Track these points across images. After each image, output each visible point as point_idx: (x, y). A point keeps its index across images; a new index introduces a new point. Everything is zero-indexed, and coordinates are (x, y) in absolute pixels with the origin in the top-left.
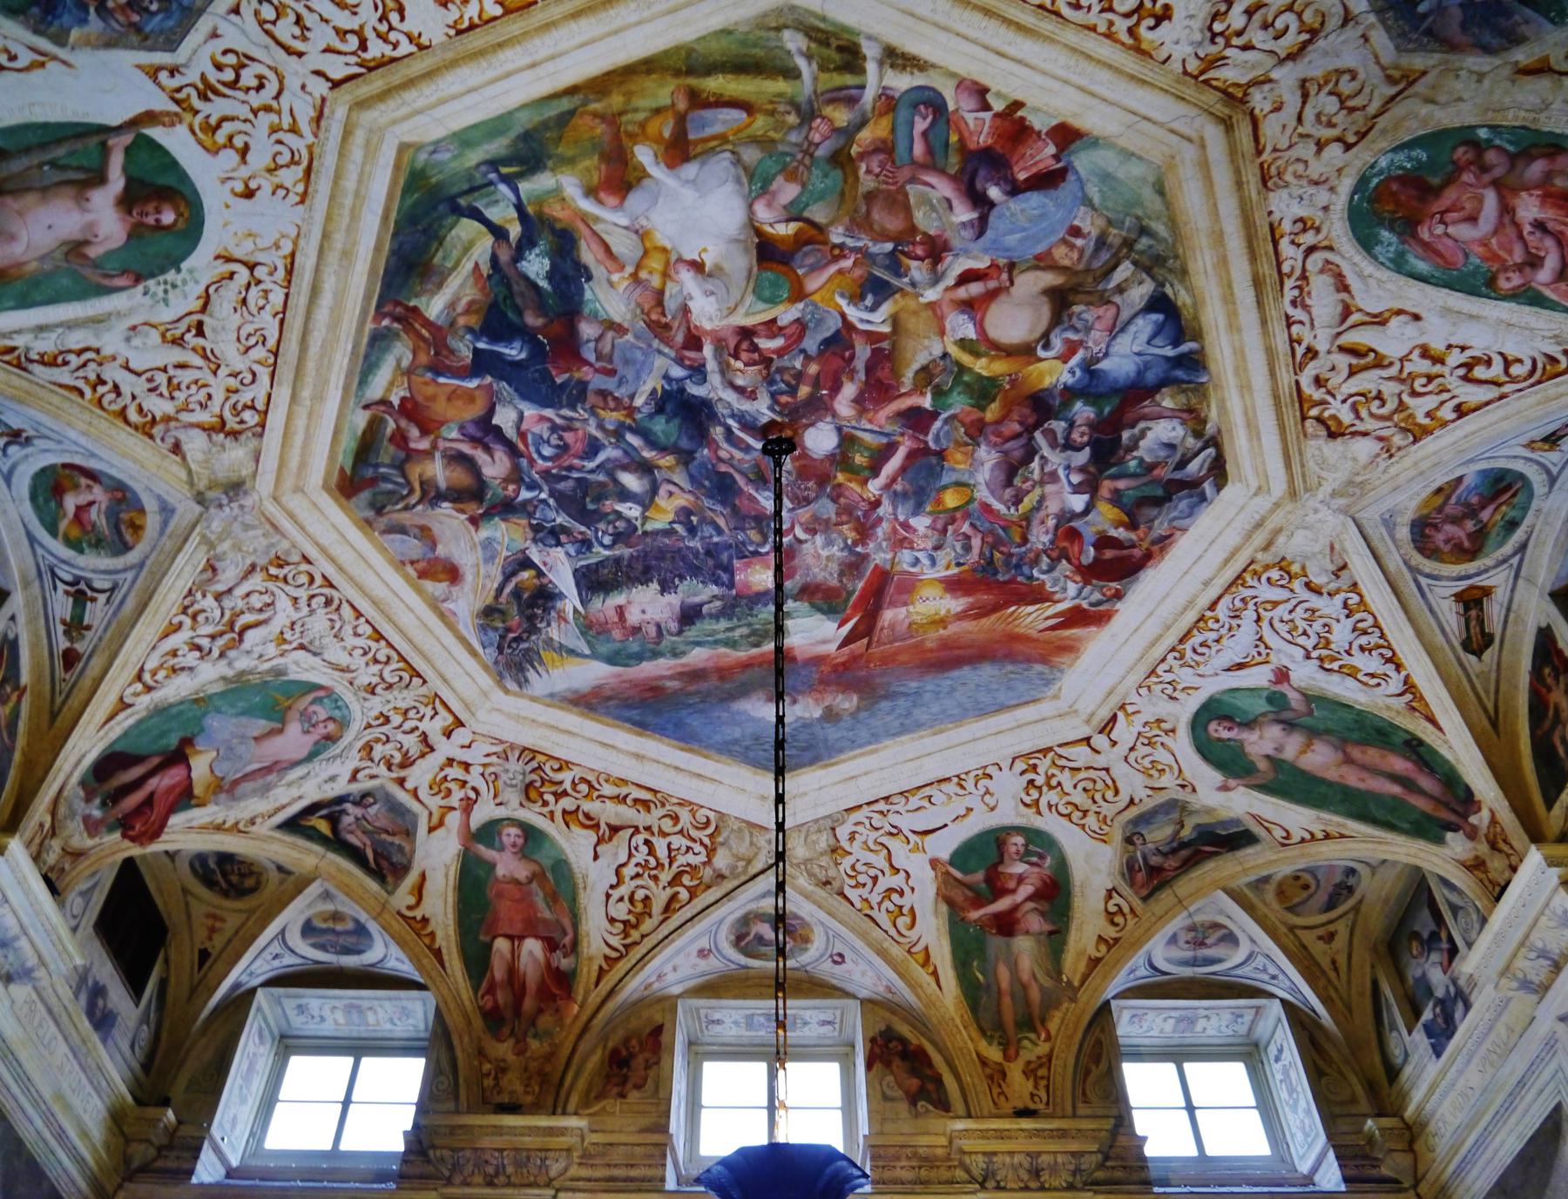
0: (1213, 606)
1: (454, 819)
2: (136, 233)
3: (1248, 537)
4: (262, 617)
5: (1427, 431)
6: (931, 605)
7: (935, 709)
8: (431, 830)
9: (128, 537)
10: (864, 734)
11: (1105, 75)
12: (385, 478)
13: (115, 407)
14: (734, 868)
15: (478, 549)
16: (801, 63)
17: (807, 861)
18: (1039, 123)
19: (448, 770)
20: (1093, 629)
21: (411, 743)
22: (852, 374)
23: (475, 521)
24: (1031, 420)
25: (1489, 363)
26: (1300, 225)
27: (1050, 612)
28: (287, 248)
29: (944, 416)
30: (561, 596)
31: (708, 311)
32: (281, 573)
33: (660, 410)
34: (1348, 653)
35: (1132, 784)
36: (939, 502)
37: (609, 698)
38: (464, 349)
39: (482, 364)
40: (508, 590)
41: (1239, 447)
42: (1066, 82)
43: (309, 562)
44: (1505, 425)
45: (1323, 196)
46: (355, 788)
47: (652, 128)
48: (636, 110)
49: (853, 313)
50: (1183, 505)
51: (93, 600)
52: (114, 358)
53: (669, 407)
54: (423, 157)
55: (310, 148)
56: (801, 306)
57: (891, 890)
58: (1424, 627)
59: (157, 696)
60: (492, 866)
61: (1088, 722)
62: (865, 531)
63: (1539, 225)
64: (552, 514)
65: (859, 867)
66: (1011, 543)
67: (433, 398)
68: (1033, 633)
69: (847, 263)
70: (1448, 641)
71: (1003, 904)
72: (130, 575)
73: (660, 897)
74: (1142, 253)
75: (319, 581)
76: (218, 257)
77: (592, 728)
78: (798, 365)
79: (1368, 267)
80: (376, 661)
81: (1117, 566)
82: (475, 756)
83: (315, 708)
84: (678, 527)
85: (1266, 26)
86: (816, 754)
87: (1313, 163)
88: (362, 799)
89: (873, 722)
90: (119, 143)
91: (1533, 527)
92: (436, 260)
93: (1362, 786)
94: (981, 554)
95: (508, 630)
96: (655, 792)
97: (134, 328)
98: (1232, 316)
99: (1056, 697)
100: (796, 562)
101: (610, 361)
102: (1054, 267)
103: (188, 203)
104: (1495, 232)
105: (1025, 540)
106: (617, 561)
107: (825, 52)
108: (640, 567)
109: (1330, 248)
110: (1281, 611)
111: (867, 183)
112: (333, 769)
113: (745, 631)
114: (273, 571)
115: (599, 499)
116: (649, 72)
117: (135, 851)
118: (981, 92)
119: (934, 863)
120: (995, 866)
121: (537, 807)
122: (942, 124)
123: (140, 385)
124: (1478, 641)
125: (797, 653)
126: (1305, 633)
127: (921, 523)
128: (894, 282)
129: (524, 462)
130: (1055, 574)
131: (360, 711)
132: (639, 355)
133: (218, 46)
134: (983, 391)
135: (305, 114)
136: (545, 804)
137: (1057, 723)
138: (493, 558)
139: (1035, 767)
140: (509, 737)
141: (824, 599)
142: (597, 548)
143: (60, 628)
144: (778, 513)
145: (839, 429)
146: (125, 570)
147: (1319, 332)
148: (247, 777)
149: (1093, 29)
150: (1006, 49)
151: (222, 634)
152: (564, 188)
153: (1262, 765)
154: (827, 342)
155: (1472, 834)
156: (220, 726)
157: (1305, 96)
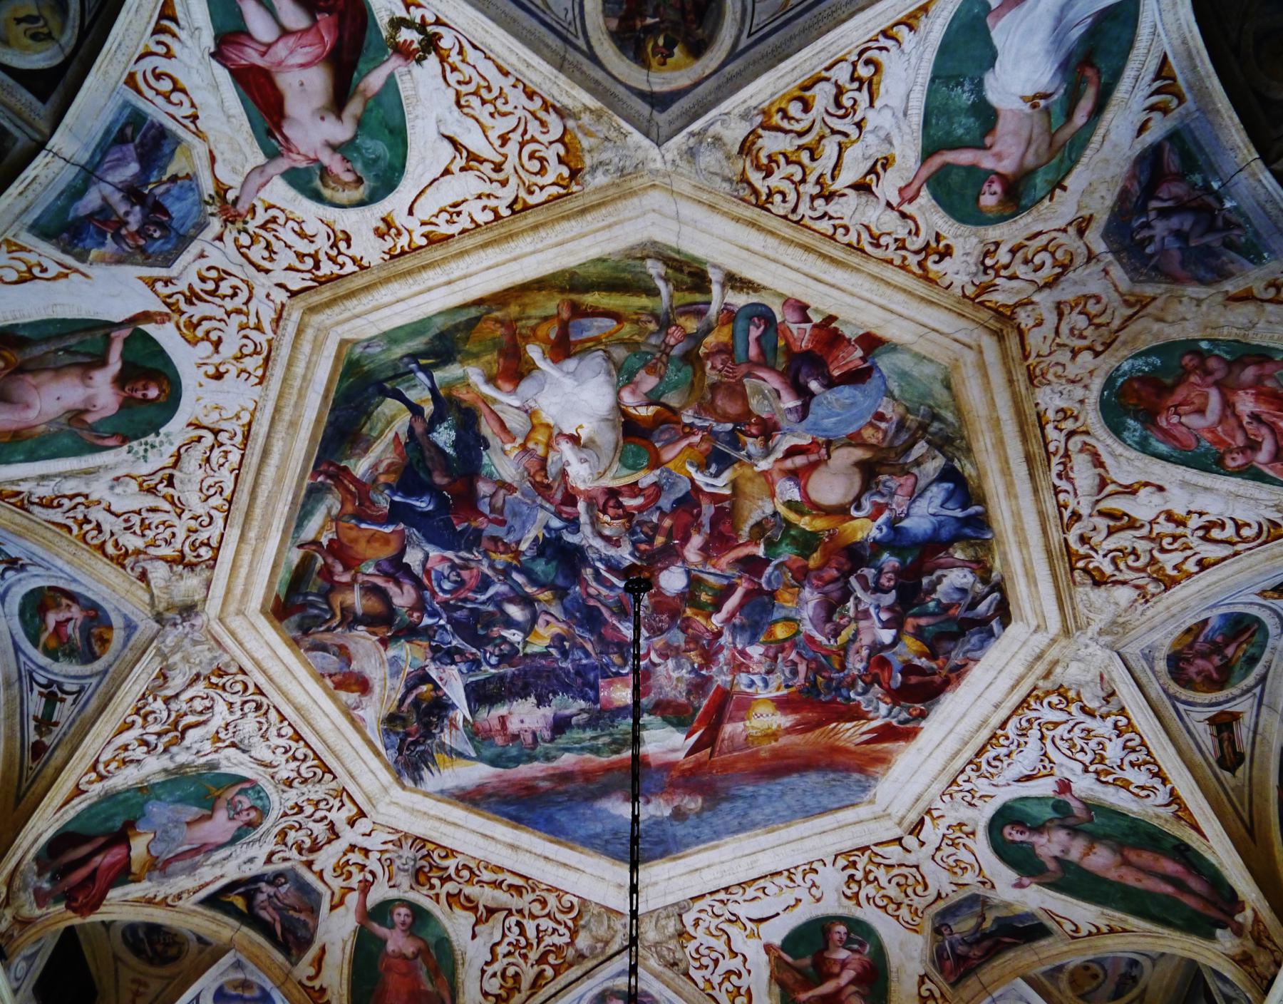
0: (1003, 726)
1: (353, 899)
2: (127, 404)
3: (1031, 667)
4: (202, 718)
6: (766, 719)
7: (768, 810)
8: (333, 908)
9: (96, 649)
10: (707, 830)
11: (901, 297)
12: (313, 605)
13: (96, 542)
14: (593, 948)
16: (660, 284)
17: (656, 944)
18: (849, 332)
19: (350, 855)
21: (320, 830)
23: (384, 642)
25: (1223, 526)
26: (1061, 415)
27: (865, 728)
28: (246, 418)
29: (775, 563)
30: (453, 707)
31: (580, 474)
32: (221, 681)
34: (1120, 767)
35: (939, 880)
36: (771, 634)
37: (490, 796)
38: (383, 502)
39: (397, 513)
40: (409, 701)
41: (1020, 591)
43: (244, 673)
44: (1239, 577)
45: (1079, 392)
46: (270, 869)
47: (541, 332)
48: (529, 318)
49: (700, 479)
50: (974, 640)
51: (63, 700)
52: (99, 503)
53: (548, 552)
54: (358, 350)
55: (270, 341)
57: (729, 972)
58: (1184, 747)
59: (108, 784)
60: (384, 942)
61: (899, 824)
62: (709, 657)
63: (1255, 417)
64: (449, 638)
65: (702, 950)
66: (832, 668)
67: (355, 540)
68: (851, 746)
69: (696, 439)
70: (1206, 759)
71: (828, 987)
72: (94, 681)
73: (529, 973)
75: (251, 689)
76: (189, 425)
77: (476, 821)
78: (655, 519)
79: (1119, 449)
80: (295, 759)
81: (921, 691)
82: (374, 843)
83: (239, 798)
84: (552, 650)
85: (1026, 262)
86: (666, 848)
87: (1069, 366)
88: (275, 879)
89: (715, 821)
90: (119, 336)
91: (1270, 662)
92: (364, 430)
94: (806, 678)
95: (408, 734)
96: (527, 879)
97: (117, 479)
98: (1010, 486)
99: (871, 802)
101: (501, 512)
104: (1220, 422)
105: (843, 667)
106: (502, 678)
107: (680, 276)
108: (520, 684)
109: (1087, 433)
110: (1062, 730)
112: (254, 851)
113: (607, 739)
114: (214, 680)
115: (488, 626)
116: (540, 290)
117: (77, 921)
118: (802, 309)
119: (768, 948)
120: (822, 952)
121: (425, 890)
122: (771, 332)
123: (118, 524)
124: (1230, 758)
125: (651, 760)
126: (1082, 750)
130: (869, 696)
131: (278, 801)
134: (807, 543)
135: (267, 316)
136: (432, 887)
137: (873, 825)
138: (398, 673)
139: (854, 863)
140: (404, 827)
141: (676, 715)
142: (485, 667)
143: (32, 724)
144: (636, 642)
145: (688, 572)
146: (90, 676)
147: (1082, 500)
148: (178, 857)
149: (891, 262)
151: (167, 732)
152: (471, 376)
153: (1052, 865)
155: (1238, 931)
156: (159, 811)
157: (1061, 315)
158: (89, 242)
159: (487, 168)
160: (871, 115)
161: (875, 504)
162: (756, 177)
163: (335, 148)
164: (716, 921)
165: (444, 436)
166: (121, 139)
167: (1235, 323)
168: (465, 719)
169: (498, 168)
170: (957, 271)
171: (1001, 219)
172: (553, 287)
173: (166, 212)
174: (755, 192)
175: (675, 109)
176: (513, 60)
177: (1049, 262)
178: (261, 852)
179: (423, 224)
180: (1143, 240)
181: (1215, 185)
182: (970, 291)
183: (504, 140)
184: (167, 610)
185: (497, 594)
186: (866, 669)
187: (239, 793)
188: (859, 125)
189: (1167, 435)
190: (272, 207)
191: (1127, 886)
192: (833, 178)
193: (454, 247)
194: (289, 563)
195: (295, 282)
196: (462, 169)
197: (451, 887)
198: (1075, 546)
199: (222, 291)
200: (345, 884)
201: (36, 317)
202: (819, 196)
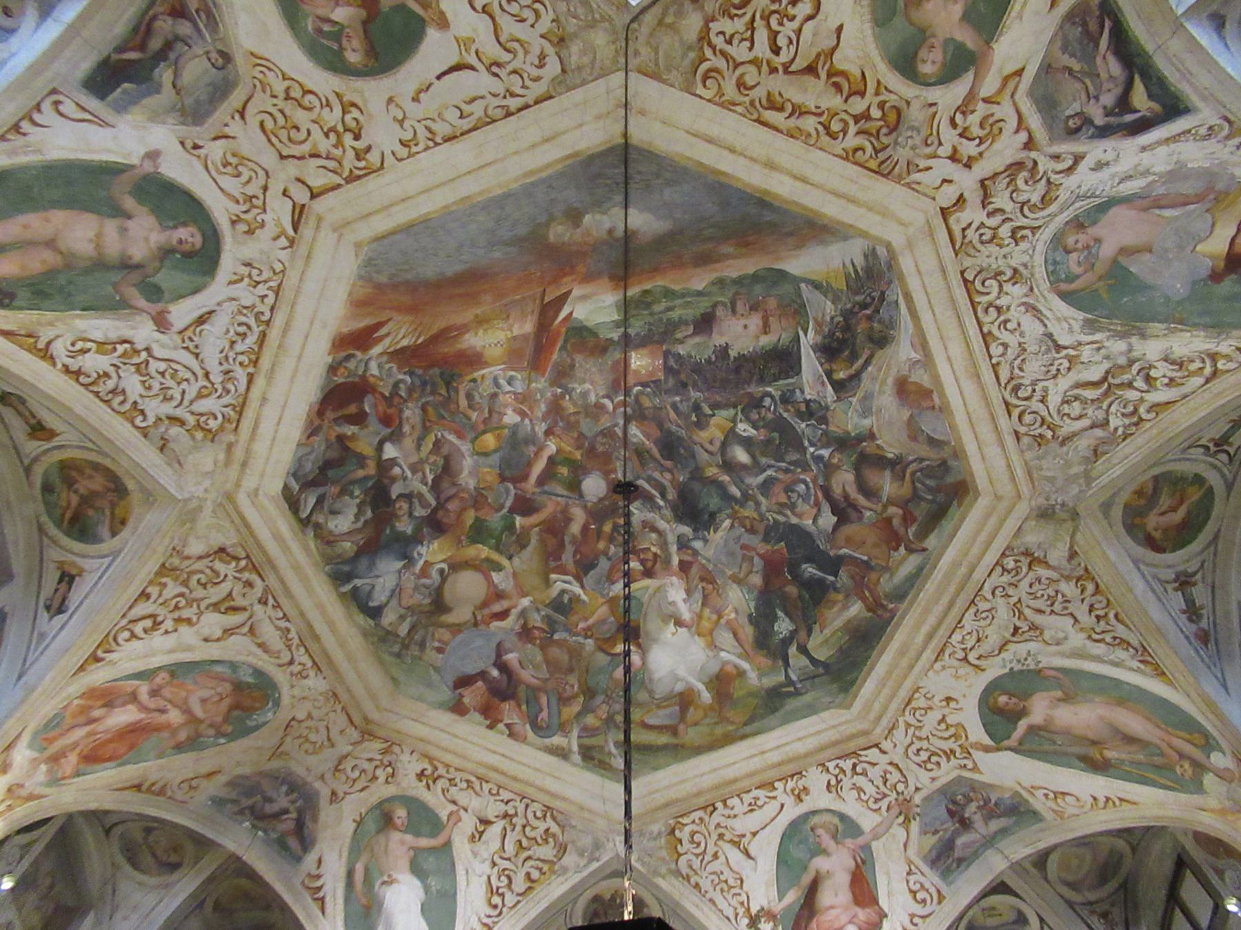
0: (251, 378)
1: (989, 87)
2: (1026, 696)
3: (248, 452)
6: (493, 338)
8: (1019, 73)
9: (1150, 486)
12: (930, 490)
13: (1099, 597)
15: (877, 413)
16: (614, 750)
17: (592, 25)
18: (477, 717)
20: (345, 330)
21: (1001, 200)
22: (574, 541)
23: (872, 436)
24: (441, 513)
26: (304, 674)
27: (387, 341)
28: (938, 666)
29: (505, 510)
30: (817, 348)
31: (676, 592)
33: (712, 515)
35: (248, 139)
36: (498, 437)
37: (791, 234)
39: (833, 565)
40: (861, 362)
41: (284, 524)
42: (466, 740)
43: (1016, 433)
45: (296, 692)
46: (1078, 147)
47: (701, 713)
49: (577, 590)
50: (308, 466)
51: (1212, 440)
52: (1082, 629)
56: (611, 594)
59: (1210, 346)
60: (966, 17)
61: (320, 219)
62: (555, 408)
63: (163, 711)
64: (808, 431)
65: (527, 14)
67: (876, 545)
69: (582, 625)
74: (395, 642)
75: (1015, 413)
78: (612, 548)
80: (999, 309)
81: (342, 398)
83: (1077, 270)
85: (364, 771)
88: (1079, 127)
93: (22, 219)
94: (457, 391)
95: (869, 318)
96: (759, 121)
97: (1058, 644)
99: (358, 245)
100: (611, 378)
101: (744, 558)
105: (424, 409)
106: (762, 381)
108: (743, 372)
109: (280, 666)
110: (192, 391)
113: (657, 308)
114: (1049, 434)
115: (769, 442)
118: (512, 735)
126: (163, 374)
128: (550, 612)
129: (821, 482)
130: (391, 381)
131: (1032, 254)
133: (931, 774)
134: (479, 533)
135: (899, 734)
136: (881, 106)
139: (358, 158)
140: (899, 190)
141: (584, 339)
142: (777, 394)
144: (627, 419)
145: (581, 496)
149: (457, 769)
150: (503, 759)
152: (756, 675)
153: (129, 203)
156: (1173, 280)
157: (329, 739)
158: (1008, 802)
160: (488, 871)
161: (428, 577)
162: (555, 829)
163: (825, 852)
165: (783, 626)
166: (960, 861)
167: (207, 760)
169: (721, 836)
170: (410, 765)
173: (949, 810)
174: (554, 818)
175: (608, 871)
176: (706, 910)
177: (349, 770)
178: (1084, 179)
179: (775, 798)
180: (292, 791)
181: (260, 833)
182: (396, 749)
183: (716, 856)
184: (1064, 520)
185: (757, 475)
186: (401, 411)
187: (1078, 277)
188: (494, 864)
190: (875, 811)
192: (505, 829)
193: (757, 779)
195: (873, 754)
196: (744, 836)
197: (858, 106)
198: (254, 577)
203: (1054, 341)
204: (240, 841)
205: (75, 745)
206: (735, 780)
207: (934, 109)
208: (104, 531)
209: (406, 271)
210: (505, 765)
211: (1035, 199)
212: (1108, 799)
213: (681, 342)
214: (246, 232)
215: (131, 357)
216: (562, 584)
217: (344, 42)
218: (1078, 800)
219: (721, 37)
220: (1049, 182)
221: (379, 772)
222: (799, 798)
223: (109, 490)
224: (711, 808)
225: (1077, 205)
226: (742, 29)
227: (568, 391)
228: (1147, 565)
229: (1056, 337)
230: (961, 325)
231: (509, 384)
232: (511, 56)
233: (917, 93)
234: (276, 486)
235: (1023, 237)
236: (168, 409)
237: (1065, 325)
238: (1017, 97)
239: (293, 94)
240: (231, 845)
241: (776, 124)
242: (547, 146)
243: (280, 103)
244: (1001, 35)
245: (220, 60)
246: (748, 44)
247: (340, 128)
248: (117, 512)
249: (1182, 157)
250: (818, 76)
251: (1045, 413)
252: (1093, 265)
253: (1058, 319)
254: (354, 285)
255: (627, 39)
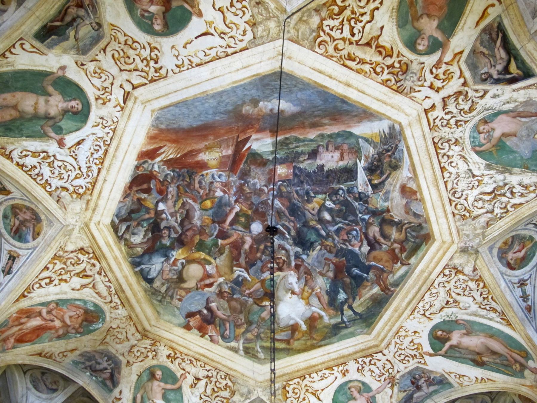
0: (99, 170)
1: (448, 57)
2: (450, 332)
3: (96, 205)
5: (53, 258)
7: (207, 105)
8: (461, 52)
9: (510, 240)
10: (240, 93)
11: (180, 343)
12: (413, 237)
13: (485, 289)
14: (310, 16)
16: (259, 350)
17: (269, 19)
18: (196, 331)
20: (144, 150)
21: (451, 107)
22: (246, 252)
23: (388, 211)
24: (183, 236)
25: (46, 284)
27: (163, 156)
28: (411, 317)
29: (214, 237)
30: (365, 169)
31: (292, 278)
33: (312, 243)
35: (107, 62)
36: (213, 203)
37: (356, 116)
38: (371, 275)
39: (367, 269)
40: (385, 176)
41: (111, 238)
43: (453, 213)
45: (113, 315)
47: (301, 335)
49: (246, 275)
50: (123, 212)
53: (309, 244)
54: (365, 331)
55: (394, 338)
60: (438, 27)
61: (136, 98)
62: (240, 190)
63: (52, 321)
64: (359, 207)
65: (240, 13)
67: (387, 261)
68: (169, 144)
69: (247, 292)
75: (454, 204)
77: (367, 102)
78: (264, 256)
79: (92, 299)
80: (448, 157)
81: (140, 181)
83: (484, 142)
85: (142, 353)
88: (487, 78)
89: (234, 99)
94: (194, 180)
95: (390, 156)
97: (466, 309)
98: (127, 280)
99: (153, 111)
100: (268, 177)
102: (184, 289)
103: (432, 334)
105: (178, 187)
106: (339, 182)
108: (330, 178)
111: (242, 316)
113: (291, 146)
114: (468, 215)
115: (340, 211)
118: (212, 341)
119: (200, 14)
122: (222, 332)
125: (269, 134)
126: (60, 167)
127: (219, 193)
129: (363, 230)
130: (164, 174)
131: (465, 133)
132: (316, 264)
133: (405, 365)
134: (201, 247)
136: (399, 62)
137: (150, 97)
138: (386, 193)
139: (156, 71)
141: (256, 159)
145: (250, 232)
151: (499, 195)
153: (51, 89)
154: (254, 265)
156: (524, 149)
157: (127, 338)
158: (438, 379)
159: (310, 391)
161: (176, 266)
162: (230, 384)
164: (233, 34)
167: (72, 344)
168: (360, 161)
169: (307, 390)
170: (164, 352)
171: (154, 366)
172: (295, 350)
174: (230, 379)
177: (135, 353)
178: (488, 101)
181: (94, 378)
182: (158, 344)
183: (304, 399)
185: (334, 226)
186: (168, 188)
187: (484, 145)
188: (201, 398)
189: (78, 307)
191: (9, 92)
193: (325, 366)
194: (416, 258)
197: (389, 61)
199: (404, 356)
200: (450, 67)
201: (465, 365)
202: (210, 377)
203: (472, 173)
204: (84, 380)
205: (13, 334)
206: (315, 366)
207: (423, 65)
208: (30, 238)
209: (174, 123)
210: (208, 354)
211: (466, 108)
212: (482, 379)
213: (302, 162)
214: (102, 104)
215: (47, 159)
216: (239, 272)
217: (154, 21)
218: (469, 378)
219: (328, 27)
220: (473, 102)
221: (149, 354)
222: (344, 375)
223: (33, 219)
224: (303, 377)
225: (485, 112)
226: (338, 24)
227: (247, 182)
228: (507, 275)
229: (473, 171)
230: (431, 162)
231: (219, 178)
232: (230, 30)
233: (416, 58)
234: (108, 221)
235: (460, 125)
236: (61, 183)
237: (477, 166)
238: (460, 63)
239: (128, 43)
240: (81, 383)
241: (352, 67)
242: (244, 70)
243: (122, 47)
244: (454, 35)
245: (97, 27)
246: (340, 31)
247: (149, 58)
248: (36, 229)
249: (531, 96)
250: (371, 47)
251: (466, 205)
252: (491, 140)
253: (474, 163)
254: (149, 129)
255: (284, 26)
